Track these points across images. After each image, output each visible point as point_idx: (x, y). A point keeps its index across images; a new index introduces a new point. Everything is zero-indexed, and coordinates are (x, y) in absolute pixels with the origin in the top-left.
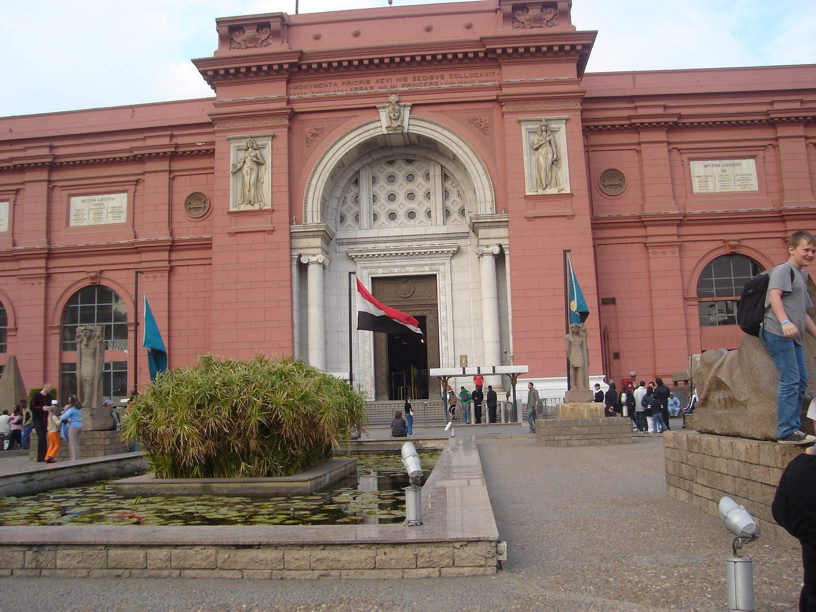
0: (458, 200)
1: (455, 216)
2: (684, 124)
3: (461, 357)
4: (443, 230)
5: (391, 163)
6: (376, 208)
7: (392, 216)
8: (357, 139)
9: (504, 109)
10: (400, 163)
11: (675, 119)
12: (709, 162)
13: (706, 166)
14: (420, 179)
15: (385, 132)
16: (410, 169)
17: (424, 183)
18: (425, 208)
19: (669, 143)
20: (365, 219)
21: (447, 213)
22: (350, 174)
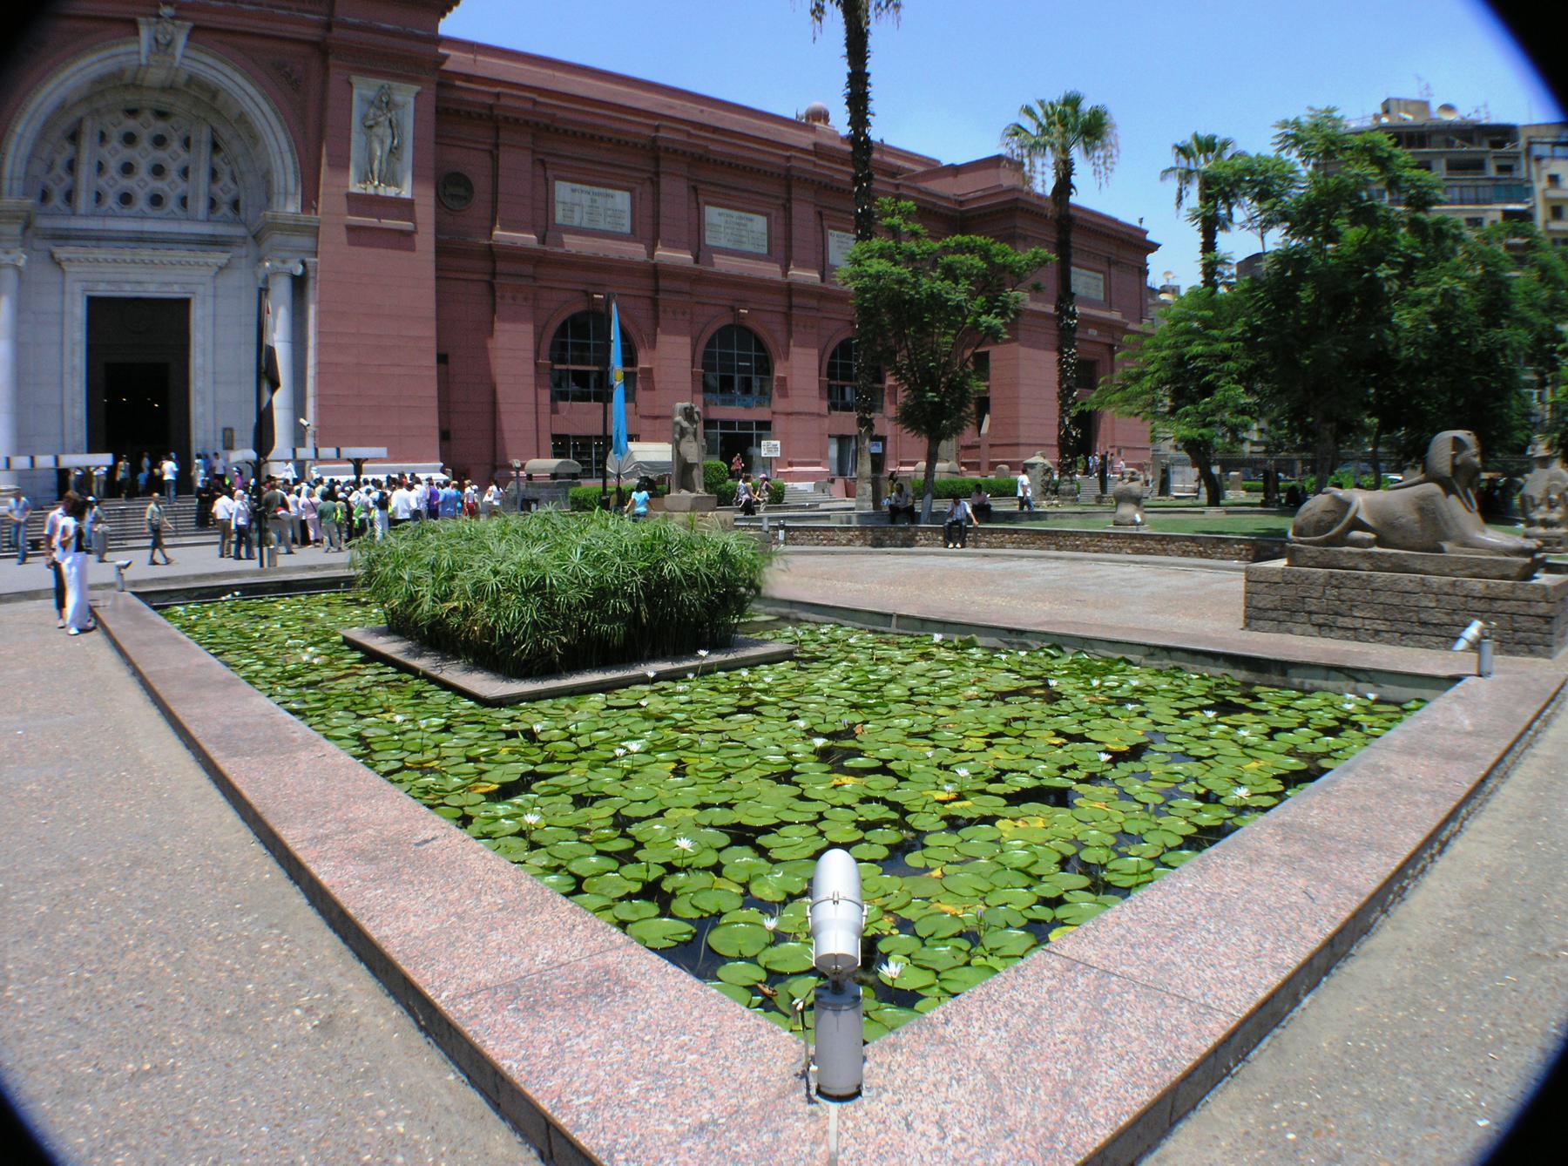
0: (232, 186)
1: (225, 210)
2: (557, 130)
3: (225, 429)
4: (206, 229)
5: (132, 113)
6: (102, 182)
7: (126, 199)
8: (97, 66)
9: (332, 60)
10: (147, 115)
11: (547, 121)
12: (578, 186)
13: (573, 191)
14: (175, 145)
15: (144, 61)
16: (159, 126)
17: (181, 151)
18: (179, 191)
19: (533, 152)
20: (84, 200)
21: (213, 204)
22: (67, 122)
